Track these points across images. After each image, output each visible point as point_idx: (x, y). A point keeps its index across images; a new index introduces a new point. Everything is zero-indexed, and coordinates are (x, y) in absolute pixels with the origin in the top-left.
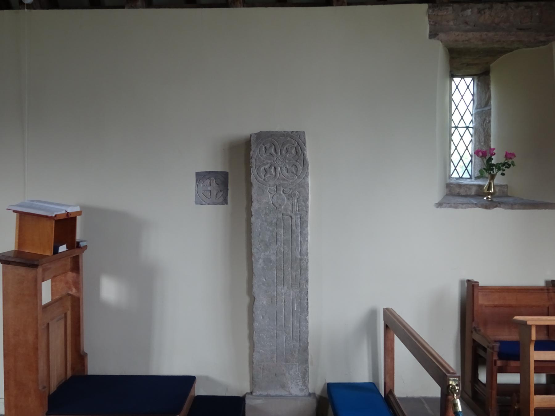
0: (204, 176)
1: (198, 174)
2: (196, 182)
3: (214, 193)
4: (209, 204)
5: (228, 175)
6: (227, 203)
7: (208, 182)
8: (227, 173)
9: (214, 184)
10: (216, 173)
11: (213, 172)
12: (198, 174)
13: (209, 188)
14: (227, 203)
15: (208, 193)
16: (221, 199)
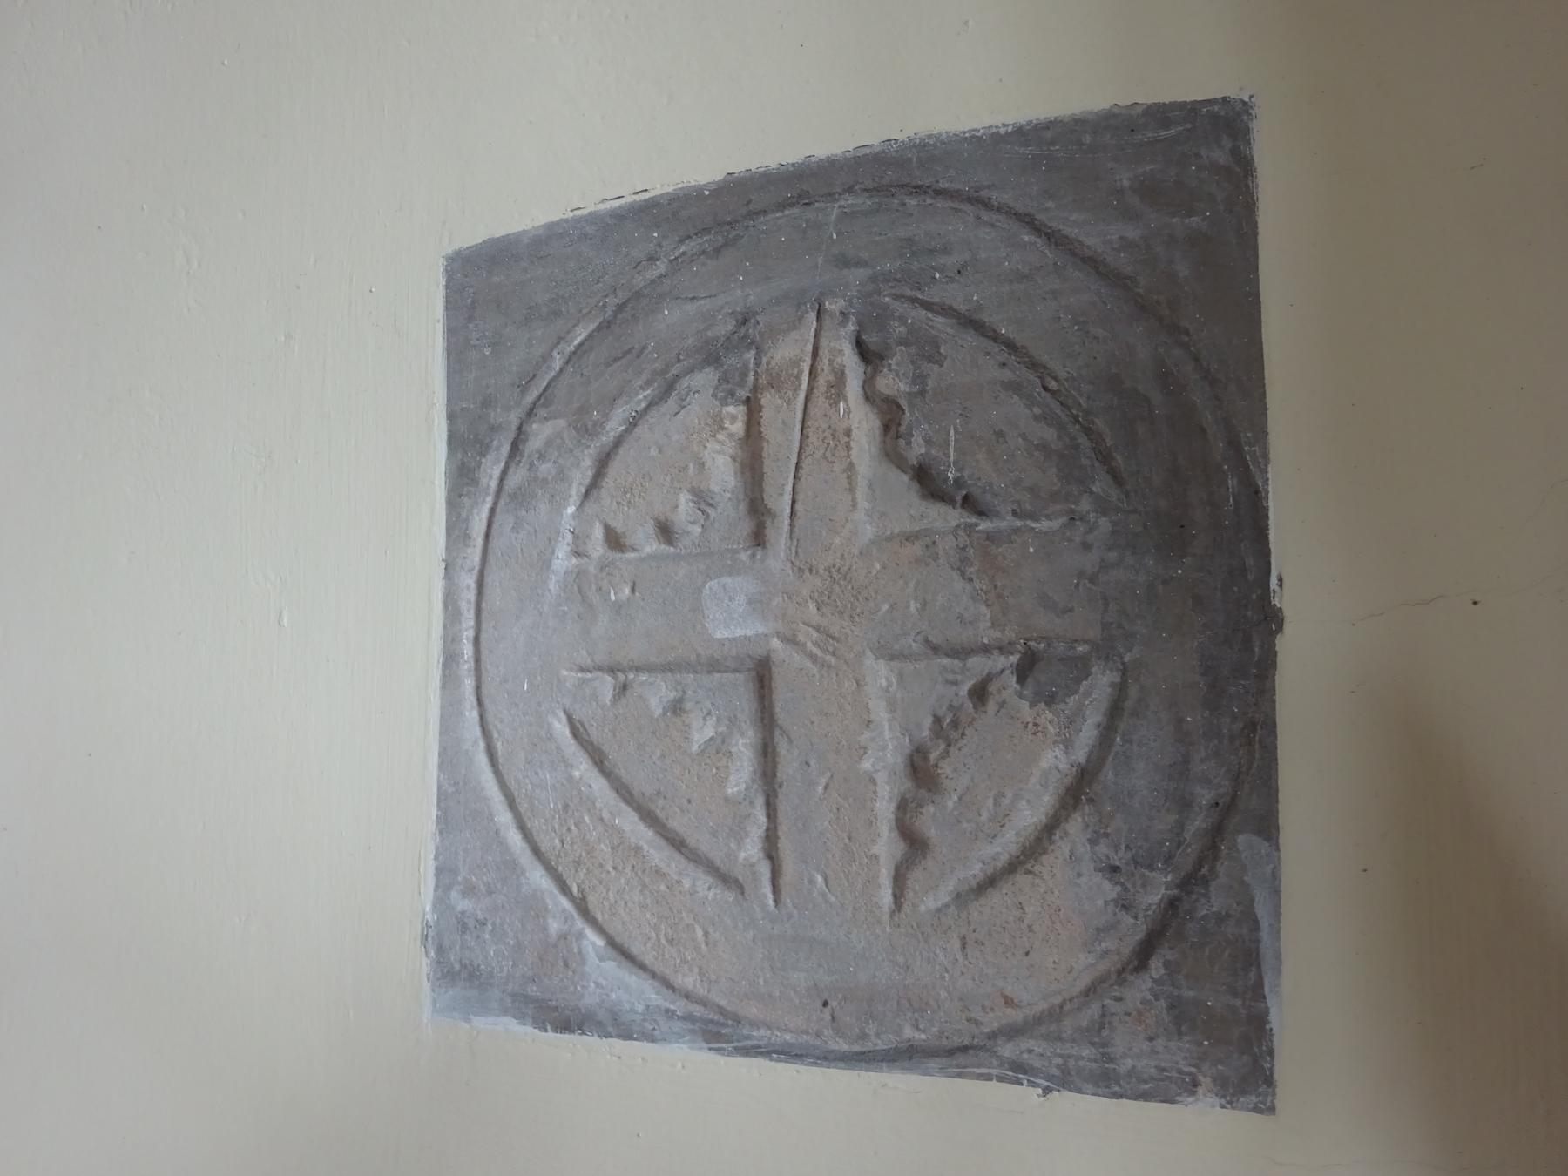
0: (631, 307)
1: (490, 289)
2: (462, 479)
3: (870, 716)
4: (719, 1030)
5: (1242, 169)
6: (1236, 1054)
7: (694, 443)
8: (1226, 122)
9: (859, 501)
10: (896, 179)
11: (800, 187)
12: (490, 289)
13: (732, 616)
14: (1236, 1054)
15: (715, 723)
16: (1065, 922)
